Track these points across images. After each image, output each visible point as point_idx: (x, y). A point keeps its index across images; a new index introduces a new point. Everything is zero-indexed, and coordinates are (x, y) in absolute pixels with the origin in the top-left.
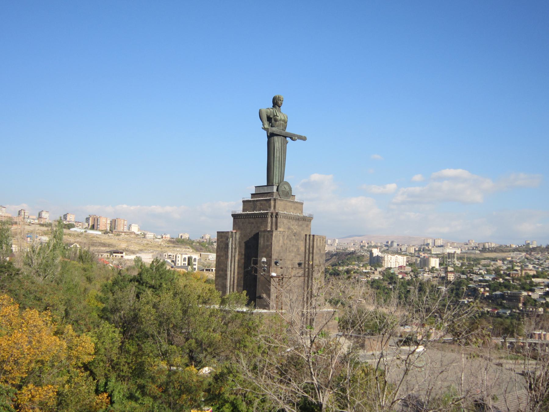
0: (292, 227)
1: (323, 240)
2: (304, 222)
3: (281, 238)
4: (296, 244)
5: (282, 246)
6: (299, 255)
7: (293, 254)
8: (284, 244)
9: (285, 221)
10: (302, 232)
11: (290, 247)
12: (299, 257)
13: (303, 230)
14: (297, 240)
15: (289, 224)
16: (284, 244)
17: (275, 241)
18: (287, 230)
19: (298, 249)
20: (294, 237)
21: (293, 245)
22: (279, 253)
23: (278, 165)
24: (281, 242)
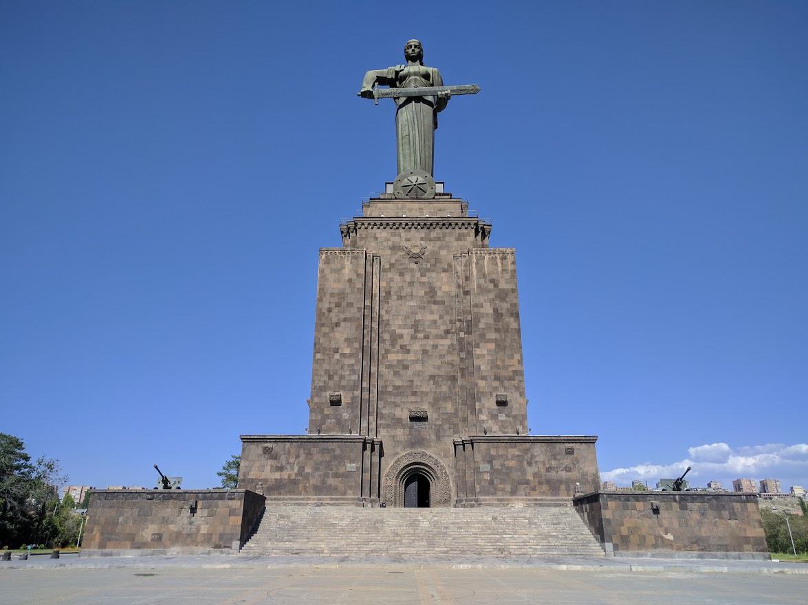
0: (404, 244)
1: (504, 258)
2: (448, 231)
3: (347, 263)
4: (424, 279)
5: (350, 281)
6: (435, 303)
7: (412, 303)
8: (358, 275)
9: (383, 234)
10: (444, 253)
11: (401, 288)
12: (435, 307)
13: (448, 247)
14: (428, 270)
15: (397, 239)
16: (358, 275)
17: (327, 271)
18: (389, 252)
19: (432, 291)
20: (413, 266)
21: (411, 284)
22: (342, 294)
23: (407, 151)
24: (347, 272)
